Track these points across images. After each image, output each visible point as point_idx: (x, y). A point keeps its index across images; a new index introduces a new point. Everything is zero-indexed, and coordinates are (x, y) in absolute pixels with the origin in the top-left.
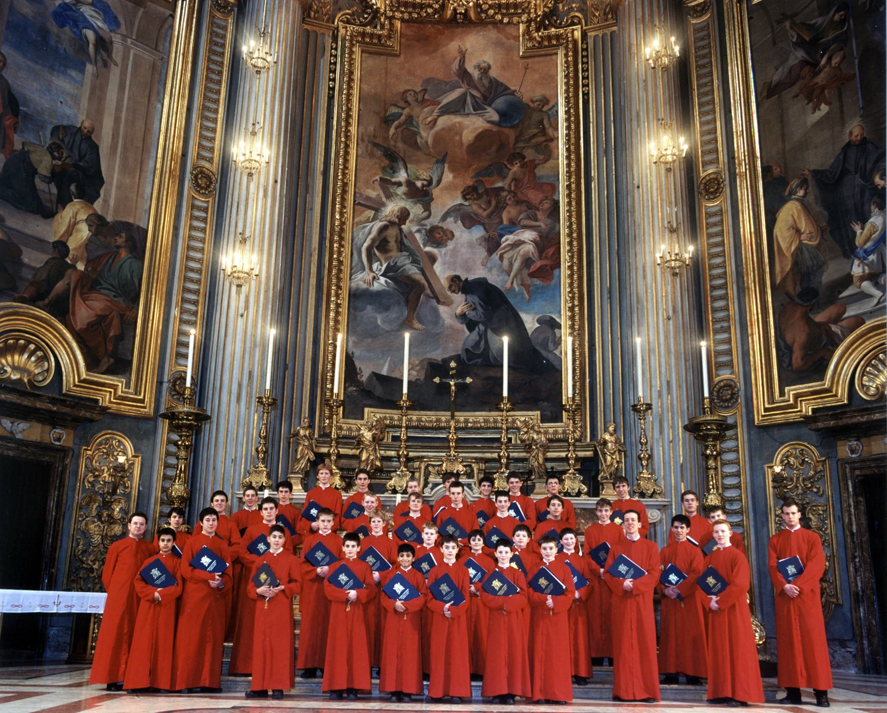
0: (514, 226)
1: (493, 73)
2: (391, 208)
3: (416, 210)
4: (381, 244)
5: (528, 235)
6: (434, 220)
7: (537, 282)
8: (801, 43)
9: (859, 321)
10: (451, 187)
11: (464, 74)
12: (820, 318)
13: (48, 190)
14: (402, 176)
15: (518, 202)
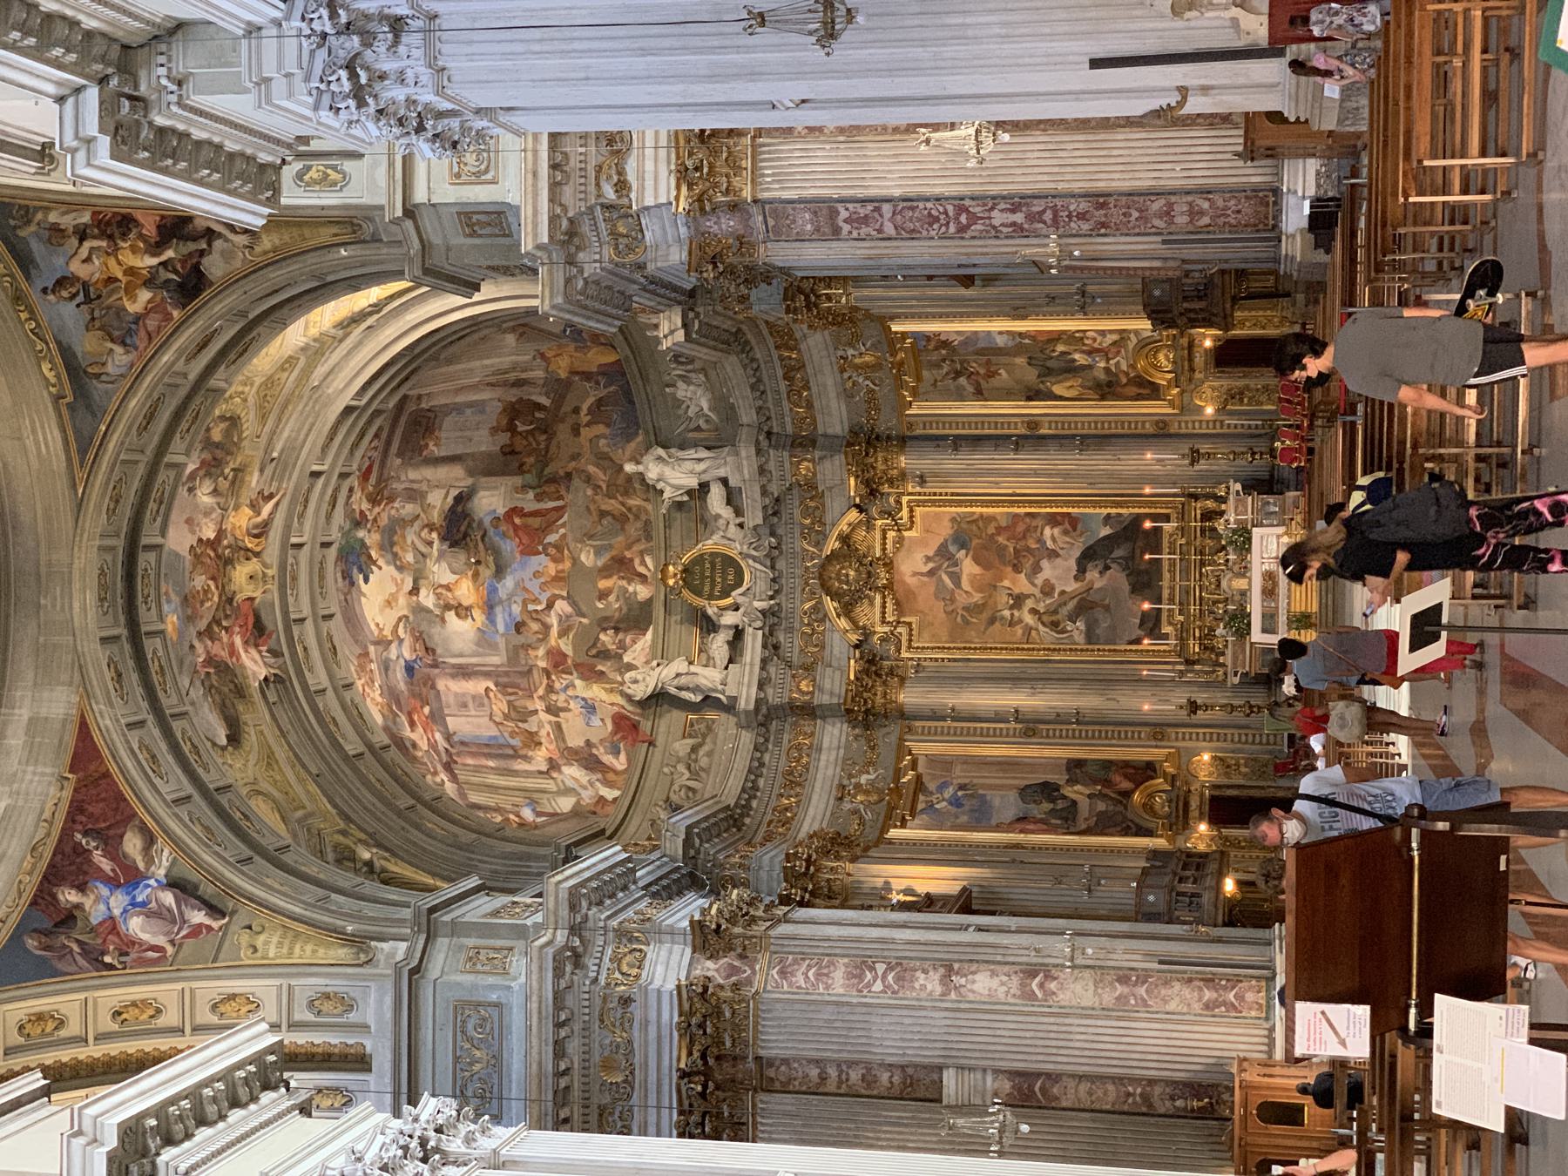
0: (1041, 541)
1: (931, 554)
2: (1029, 619)
3: (1029, 603)
4: (1054, 625)
5: (1048, 531)
6: (1037, 592)
7: (1079, 526)
8: (954, 379)
9: (1133, 366)
10: (1014, 582)
11: (931, 573)
12: (1124, 380)
13: (1060, 804)
14: (1007, 613)
15: (1024, 537)
